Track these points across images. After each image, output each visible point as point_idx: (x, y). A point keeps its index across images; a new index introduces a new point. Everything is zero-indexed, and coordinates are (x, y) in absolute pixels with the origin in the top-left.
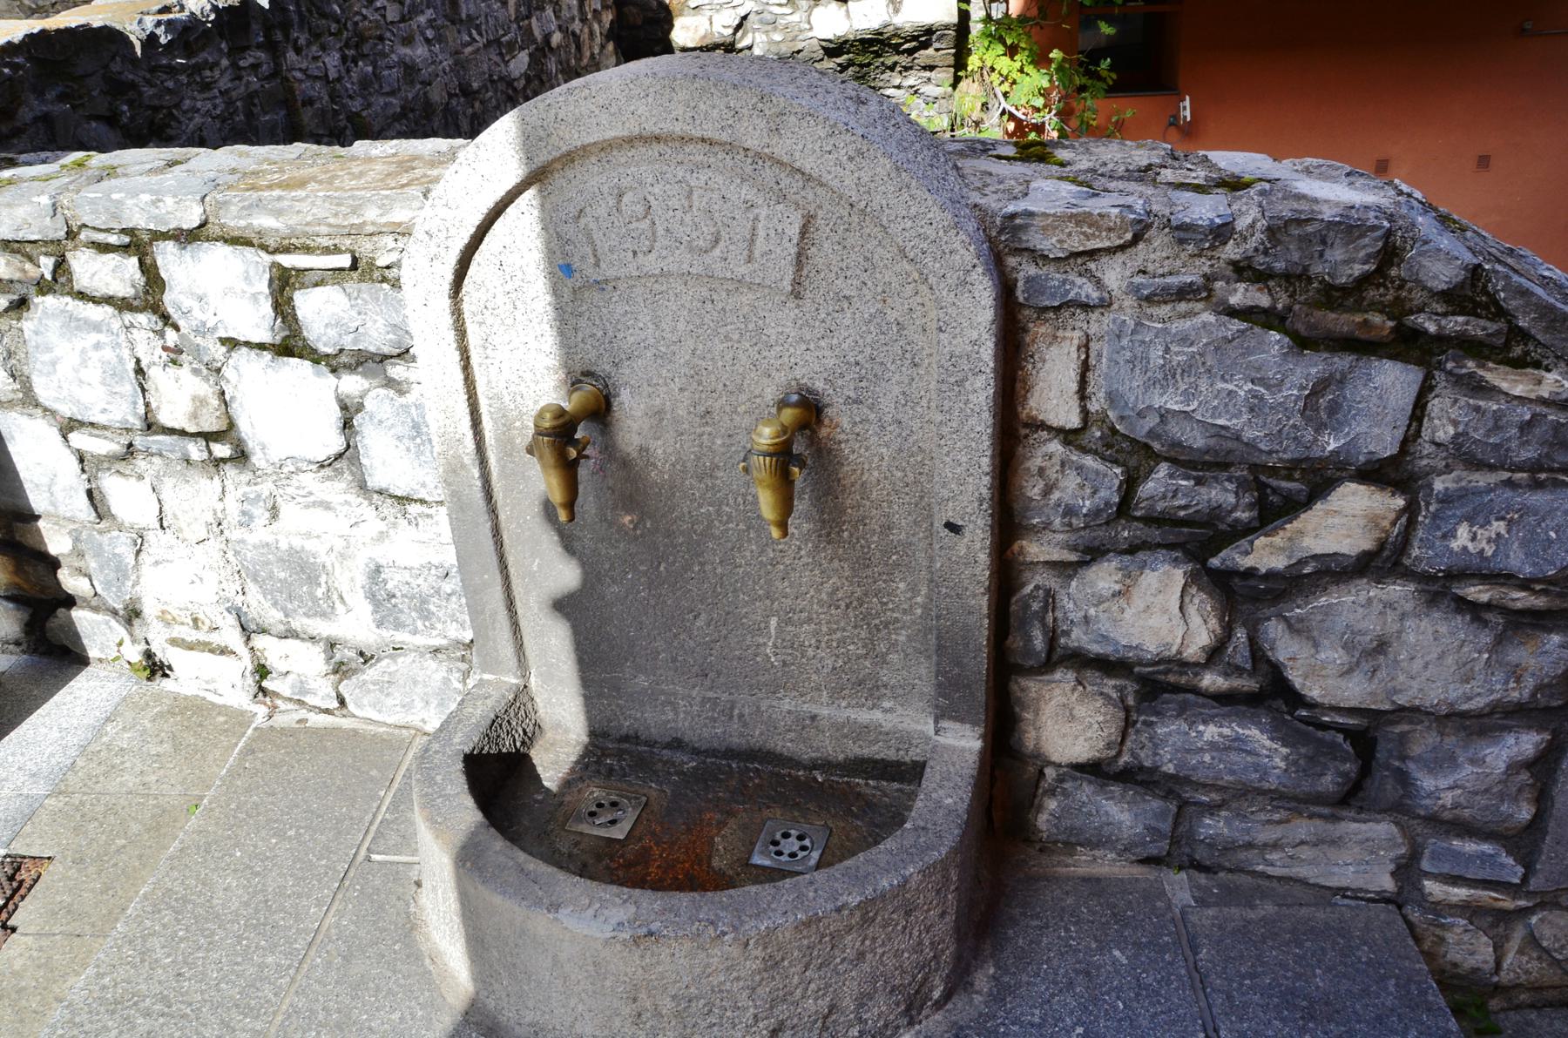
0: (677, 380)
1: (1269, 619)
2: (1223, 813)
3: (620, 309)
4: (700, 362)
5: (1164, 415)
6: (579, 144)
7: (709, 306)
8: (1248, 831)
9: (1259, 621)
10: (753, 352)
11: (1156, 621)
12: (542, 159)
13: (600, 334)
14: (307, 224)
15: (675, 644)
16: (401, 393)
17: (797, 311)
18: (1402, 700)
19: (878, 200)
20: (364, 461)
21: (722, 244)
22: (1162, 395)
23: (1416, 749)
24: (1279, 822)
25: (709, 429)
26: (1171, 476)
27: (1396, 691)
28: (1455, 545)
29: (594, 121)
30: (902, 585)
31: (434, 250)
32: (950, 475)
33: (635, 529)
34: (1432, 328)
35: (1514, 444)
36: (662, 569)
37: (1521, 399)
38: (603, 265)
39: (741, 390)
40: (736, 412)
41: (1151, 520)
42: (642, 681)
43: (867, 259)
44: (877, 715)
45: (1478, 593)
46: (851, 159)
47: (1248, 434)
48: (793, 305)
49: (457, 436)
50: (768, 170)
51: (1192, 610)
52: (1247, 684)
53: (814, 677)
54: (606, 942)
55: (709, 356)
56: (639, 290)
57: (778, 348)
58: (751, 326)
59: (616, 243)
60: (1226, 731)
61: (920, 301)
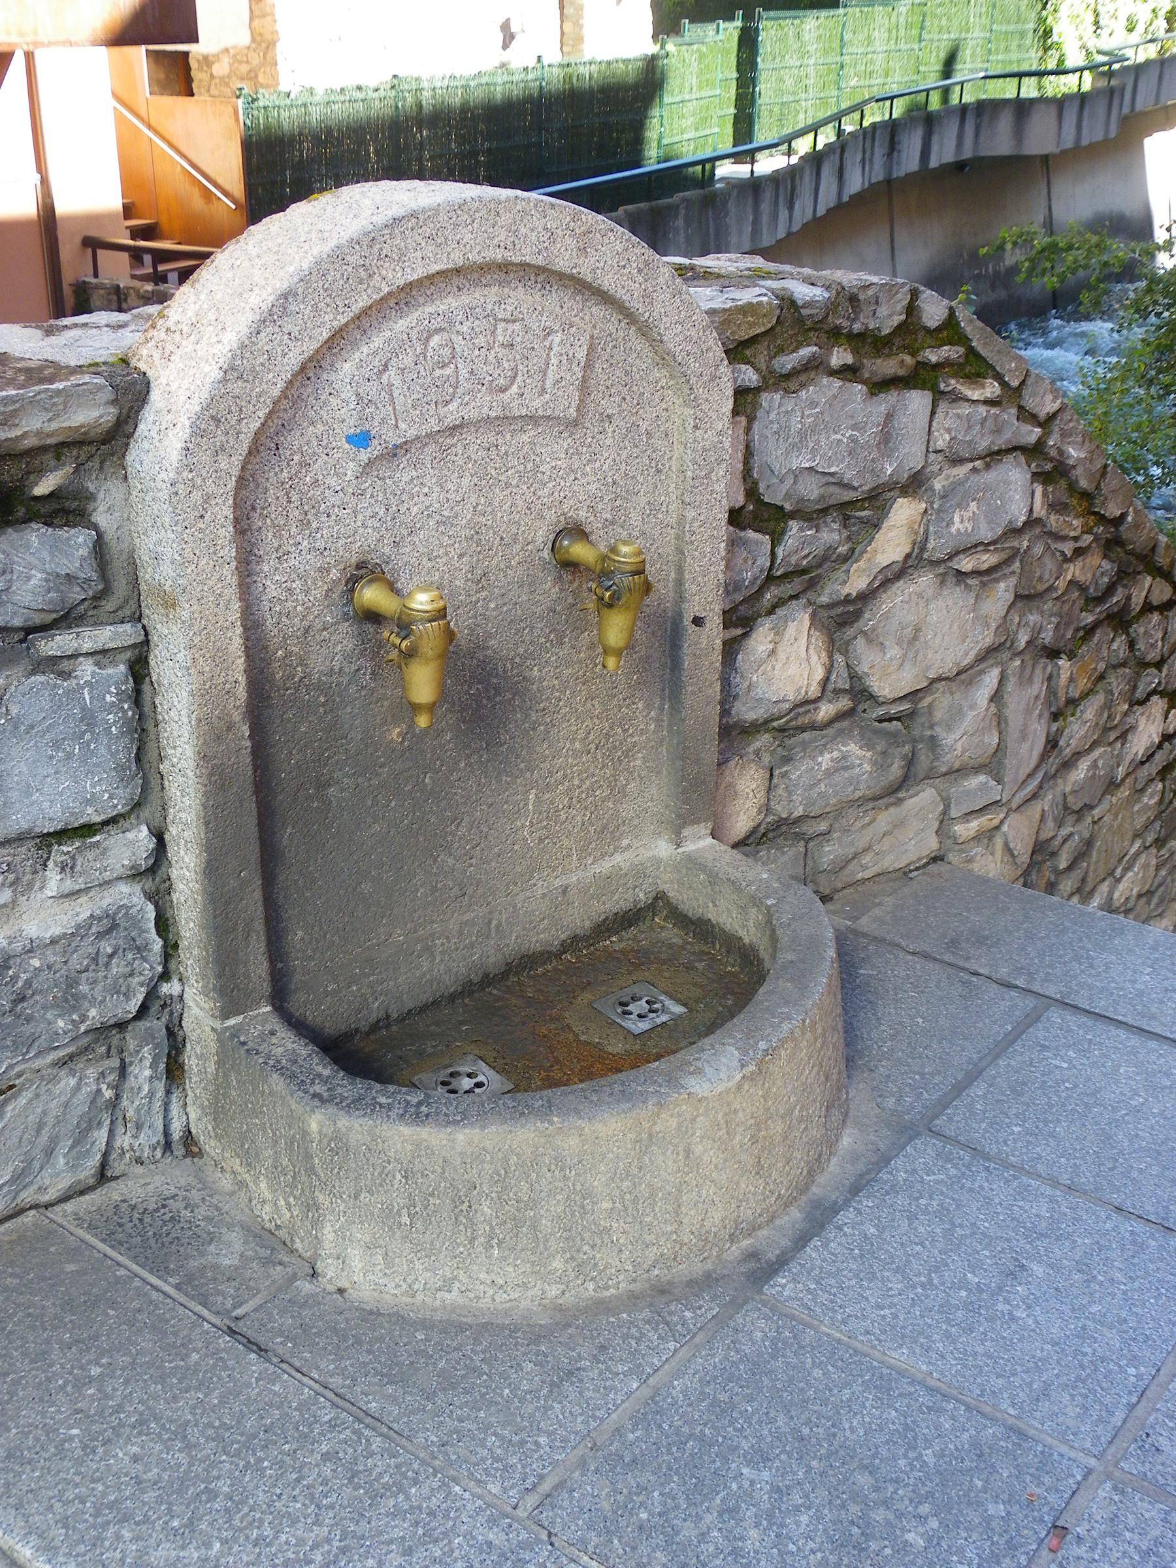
0: (457, 545)
1: (855, 638)
2: (835, 835)
3: (406, 478)
5: (797, 474)
6: (402, 282)
7: (493, 451)
8: (852, 843)
9: (848, 643)
10: (528, 495)
12: (361, 304)
15: (434, 870)
16: (66, 675)
17: (569, 440)
18: (932, 675)
19: (658, 308)
21: (519, 378)
22: (798, 457)
23: (938, 715)
24: (871, 822)
26: (801, 529)
27: (928, 668)
28: (953, 530)
29: (419, 254)
30: (640, 705)
32: (697, 569)
33: (403, 741)
36: (427, 780)
38: (403, 426)
39: (515, 540)
40: (509, 567)
42: (399, 936)
43: (627, 373)
44: (618, 858)
46: (640, 271)
47: (849, 475)
51: (811, 651)
52: (845, 703)
53: (566, 843)
54: (739, 1087)
55: (490, 509)
56: (429, 449)
57: (551, 485)
58: (530, 466)
59: (421, 395)
60: (836, 754)
61: (664, 406)
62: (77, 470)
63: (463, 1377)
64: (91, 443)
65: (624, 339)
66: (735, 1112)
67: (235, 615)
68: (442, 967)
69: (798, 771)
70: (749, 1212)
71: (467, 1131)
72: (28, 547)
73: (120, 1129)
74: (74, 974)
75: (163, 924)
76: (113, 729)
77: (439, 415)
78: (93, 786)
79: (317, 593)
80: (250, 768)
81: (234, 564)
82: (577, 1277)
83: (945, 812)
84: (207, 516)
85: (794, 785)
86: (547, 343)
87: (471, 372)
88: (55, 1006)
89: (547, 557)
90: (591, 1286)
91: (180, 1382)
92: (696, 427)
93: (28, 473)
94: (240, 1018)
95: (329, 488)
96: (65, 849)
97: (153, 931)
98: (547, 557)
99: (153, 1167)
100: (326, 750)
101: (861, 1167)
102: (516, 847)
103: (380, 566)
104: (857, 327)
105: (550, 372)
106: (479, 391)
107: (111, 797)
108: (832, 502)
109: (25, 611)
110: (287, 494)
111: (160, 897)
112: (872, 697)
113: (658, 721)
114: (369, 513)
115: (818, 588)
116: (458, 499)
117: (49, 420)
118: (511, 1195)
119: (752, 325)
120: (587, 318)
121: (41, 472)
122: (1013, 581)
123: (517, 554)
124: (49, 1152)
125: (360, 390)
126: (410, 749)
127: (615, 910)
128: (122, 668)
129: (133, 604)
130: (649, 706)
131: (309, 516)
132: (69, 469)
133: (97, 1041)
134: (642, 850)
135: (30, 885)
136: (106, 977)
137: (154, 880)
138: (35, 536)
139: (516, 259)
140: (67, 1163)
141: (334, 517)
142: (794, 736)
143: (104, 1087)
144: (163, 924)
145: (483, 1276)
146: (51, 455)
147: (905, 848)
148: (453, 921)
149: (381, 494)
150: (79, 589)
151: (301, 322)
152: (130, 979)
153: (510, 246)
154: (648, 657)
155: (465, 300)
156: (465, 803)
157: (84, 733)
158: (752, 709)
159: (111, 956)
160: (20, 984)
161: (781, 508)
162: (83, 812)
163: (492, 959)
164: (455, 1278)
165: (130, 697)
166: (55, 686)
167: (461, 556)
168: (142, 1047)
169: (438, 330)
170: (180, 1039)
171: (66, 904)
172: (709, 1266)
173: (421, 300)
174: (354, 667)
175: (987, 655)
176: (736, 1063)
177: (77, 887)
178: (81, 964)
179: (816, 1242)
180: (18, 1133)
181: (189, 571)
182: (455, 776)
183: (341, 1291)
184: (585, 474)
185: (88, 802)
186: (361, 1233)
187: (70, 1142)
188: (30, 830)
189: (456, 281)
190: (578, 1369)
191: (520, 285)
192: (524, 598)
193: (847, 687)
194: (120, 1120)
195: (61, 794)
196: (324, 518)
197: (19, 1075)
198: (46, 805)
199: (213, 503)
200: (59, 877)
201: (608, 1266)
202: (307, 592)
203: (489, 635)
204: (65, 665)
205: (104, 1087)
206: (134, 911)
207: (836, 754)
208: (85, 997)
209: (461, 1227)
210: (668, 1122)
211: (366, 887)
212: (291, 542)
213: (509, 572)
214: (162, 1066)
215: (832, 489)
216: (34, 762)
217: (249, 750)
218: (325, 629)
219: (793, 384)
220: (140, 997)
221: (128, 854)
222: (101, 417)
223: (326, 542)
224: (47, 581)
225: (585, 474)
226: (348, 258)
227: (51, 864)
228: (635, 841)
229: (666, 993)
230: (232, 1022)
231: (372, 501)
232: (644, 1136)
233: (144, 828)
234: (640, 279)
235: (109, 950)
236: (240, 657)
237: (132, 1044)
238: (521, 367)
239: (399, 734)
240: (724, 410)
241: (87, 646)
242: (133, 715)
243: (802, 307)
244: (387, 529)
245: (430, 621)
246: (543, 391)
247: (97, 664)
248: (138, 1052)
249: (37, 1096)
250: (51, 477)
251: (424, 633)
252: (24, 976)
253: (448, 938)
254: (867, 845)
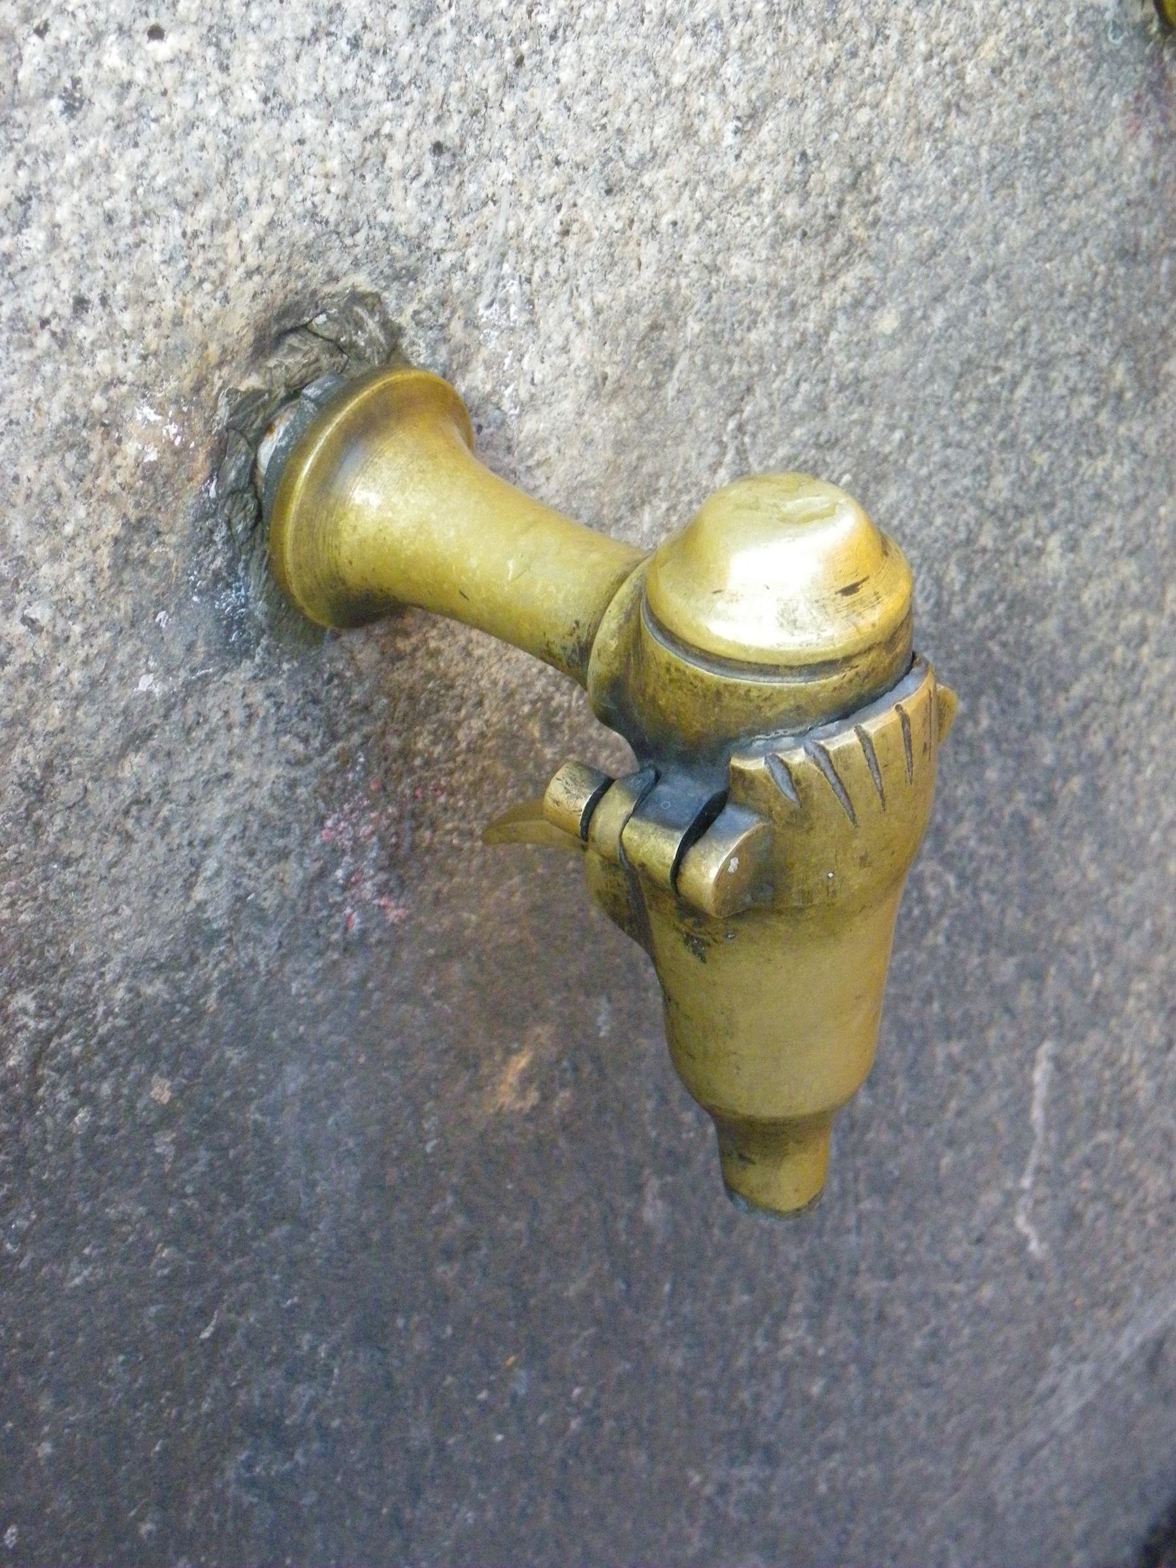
0: (730, 70)
100: (203, 1315)
103: (373, 302)
174: (294, 872)
213: (958, 126)
223: (81, 266)
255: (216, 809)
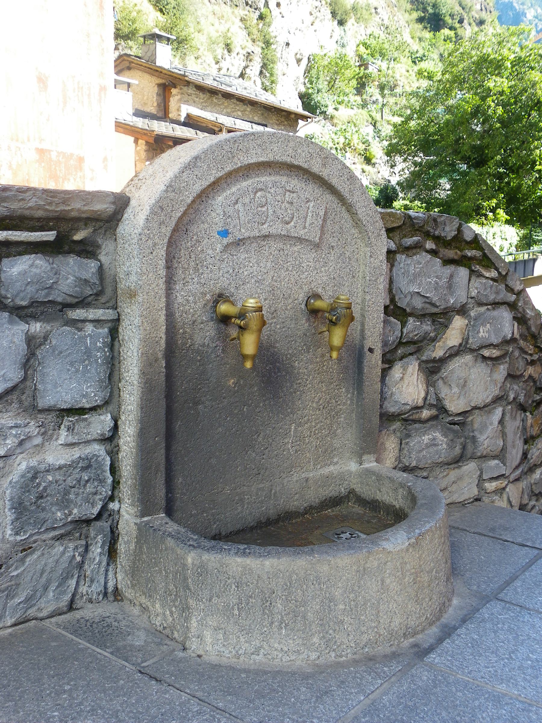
0: (264, 294)
1: (438, 380)
3: (243, 257)
4: (275, 283)
9: (435, 382)
11: (411, 389)
13: (231, 271)
14: (30, 208)
15: (246, 458)
16: (80, 330)
17: (315, 254)
19: (355, 198)
20: (39, 386)
21: (295, 219)
23: (476, 426)
24: (447, 475)
25: (275, 320)
26: (414, 321)
27: (471, 401)
28: (480, 335)
30: (343, 390)
31: (163, 218)
33: (235, 387)
34: (469, 254)
35: (489, 294)
36: (245, 410)
37: (487, 278)
38: (243, 231)
39: (290, 297)
40: (286, 309)
41: (408, 343)
43: (341, 228)
44: (332, 468)
45: (486, 353)
46: (348, 180)
47: (435, 299)
48: (314, 251)
49: (157, 339)
50: (310, 186)
51: (419, 382)
52: (434, 412)
53: (308, 455)
54: (407, 550)
55: (279, 280)
57: (306, 273)
58: (297, 262)
59: (251, 218)
60: (430, 436)
62: (95, 230)
63: (268, 693)
64: (101, 221)
65: (340, 212)
66: (406, 563)
67: (163, 304)
68: (247, 511)
69: (413, 442)
70: (413, 623)
71: (271, 560)
72: (68, 264)
73: (82, 582)
74: (68, 488)
75: (114, 470)
76: (99, 360)
77: (259, 229)
78: (87, 388)
79: (200, 304)
80: (164, 383)
81: (164, 279)
82: (326, 648)
83: (480, 476)
84: (154, 253)
85: (412, 449)
86: (307, 205)
87: (274, 212)
88: (57, 504)
89: (303, 307)
90: (333, 654)
91: (114, 693)
92: (371, 256)
93: (72, 229)
94: (150, 518)
95: (208, 255)
96: (70, 419)
97: (109, 472)
98: (303, 307)
99: (98, 604)
100: (199, 384)
101: (465, 612)
102: (285, 453)
103: (229, 297)
104: (437, 233)
105: (308, 219)
106: (277, 221)
107: (95, 396)
108: (427, 312)
109: (64, 295)
110: (190, 253)
111: (113, 453)
112: (446, 411)
113: (352, 400)
114: (225, 270)
115: (421, 352)
116: (265, 272)
117: (84, 205)
118: (293, 597)
119: (393, 222)
120: (324, 199)
121: (77, 230)
122: (506, 365)
123: (290, 304)
124: (46, 588)
125: (225, 210)
126: (237, 391)
127: (330, 495)
128: (106, 330)
129: (113, 301)
130: (347, 391)
131: (199, 266)
132: (91, 230)
133: (75, 529)
134: (343, 466)
135: (52, 435)
136: (83, 492)
137: (111, 445)
138: (72, 260)
139: (296, 163)
140: (54, 596)
141: (210, 269)
142: (411, 425)
143: (77, 554)
144: (114, 470)
145: (276, 645)
146: (83, 223)
147: (463, 491)
148: (254, 487)
149: (231, 263)
150: (89, 289)
151: (202, 171)
152: (95, 496)
153: (293, 157)
154: (347, 367)
155: (273, 178)
156: (262, 425)
157: (85, 360)
158: (393, 406)
159: (87, 481)
160: (41, 488)
161: (405, 310)
162: (81, 401)
163: (271, 511)
164: (261, 647)
165: (108, 345)
166: (74, 334)
167: (265, 300)
168: (97, 535)
169: (261, 190)
170: (116, 535)
171: (68, 450)
172: (394, 649)
173: (254, 176)
174: (214, 345)
175: (497, 400)
176: (405, 537)
177: (74, 441)
178: (72, 483)
179: (448, 640)
180: (31, 574)
181: (144, 278)
182: (258, 410)
183: (199, 656)
184: (321, 272)
185: (84, 396)
186: (212, 622)
187: (57, 584)
188: (55, 406)
189: (269, 170)
190: (331, 691)
191: (296, 178)
192: (293, 326)
193: (435, 403)
194: (83, 577)
195: (71, 390)
196: (205, 269)
197: (35, 542)
198: (64, 394)
199: (157, 247)
200: (66, 434)
201: (342, 643)
202: (195, 303)
203: (277, 341)
204: (80, 325)
205: (77, 554)
206: (100, 459)
207: (430, 436)
208: (72, 501)
209: (266, 616)
210: (373, 563)
211: (213, 461)
212: (190, 277)
213: (286, 312)
214: (107, 548)
215: (427, 306)
216: (60, 371)
217: (164, 374)
218: (202, 323)
219: (410, 253)
220: (99, 507)
221: (100, 427)
222: (107, 208)
223: (205, 281)
224: (75, 281)
225: (321, 272)
226: (224, 147)
227: (62, 427)
228: (340, 460)
229: (358, 531)
230: (145, 519)
231: (227, 265)
232: (361, 569)
233: (109, 415)
234: (348, 183)
235: (86, 478)
236: (164, 326)
237: (92, 534)
238: (295, 214)
239: (233, 383)
240: (383, 251)
241: (91, 317)
242: (109, 355)
243: (414, 219)
244: (233, 280)
245: (255, 312)
246: (305, 228)
247: (95, 327)
248: (95, 538)
249: (43, 554)
250: (82, 232)
251: (252, 317)
252: (44, 484)
253: (251, 495)
254: (445, 486)
255: (208, 334)
